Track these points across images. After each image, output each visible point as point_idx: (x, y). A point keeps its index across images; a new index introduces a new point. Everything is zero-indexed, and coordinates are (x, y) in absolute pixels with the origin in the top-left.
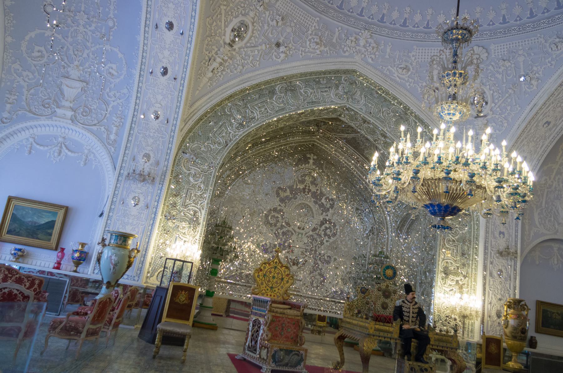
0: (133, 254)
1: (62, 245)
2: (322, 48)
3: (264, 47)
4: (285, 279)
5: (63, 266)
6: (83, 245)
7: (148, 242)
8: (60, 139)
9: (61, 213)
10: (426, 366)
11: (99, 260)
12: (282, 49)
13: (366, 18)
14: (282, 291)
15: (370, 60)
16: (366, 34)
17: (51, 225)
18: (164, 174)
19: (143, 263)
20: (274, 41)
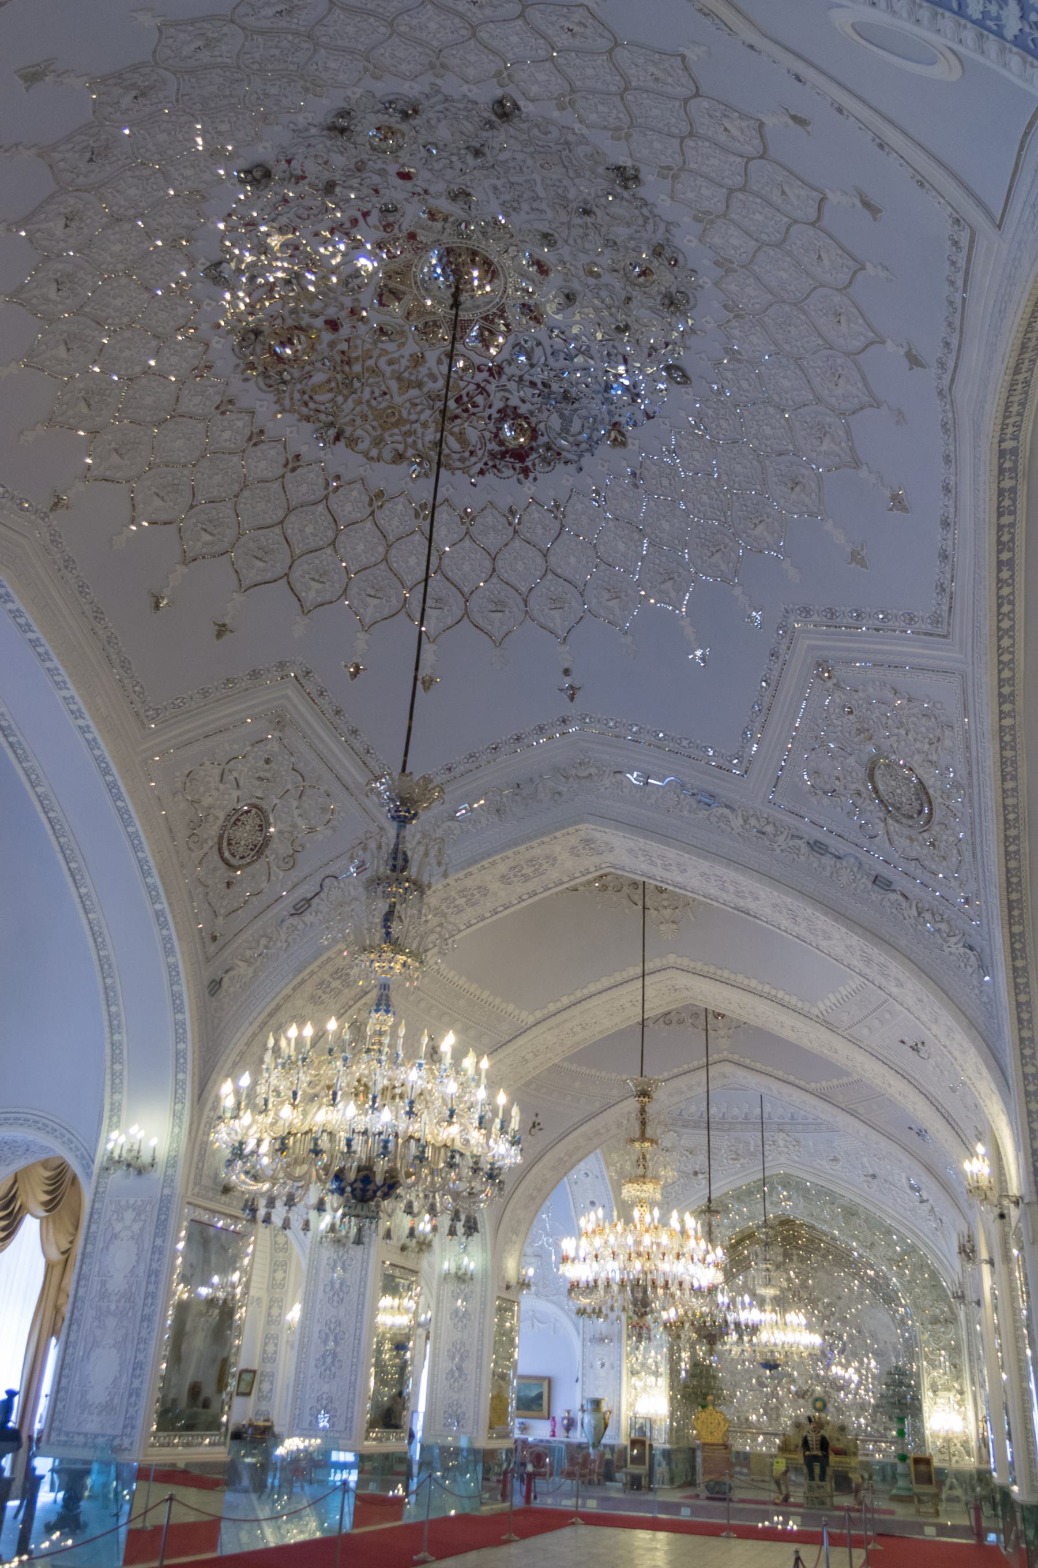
0: (607, 1416)
1: (552, 1415)
2: (742, 1161)
3: (682, 1180)
4: (722, 1423)
5: (557, 1433)
6: (569, 1412)
7: (620, 1402)
8: (531, 1313)
9: (546, 1384)
10: (822, 1483)
11: (582, 1425)
12: (700, 1176)
13: (776, 1120)
14: (721, 1435)
15: (796, 1158)
16: (782, 1135)
17: (540, 1396)
18: (620, 1332)
19: (619, 1421)
20: (691, 1172)
